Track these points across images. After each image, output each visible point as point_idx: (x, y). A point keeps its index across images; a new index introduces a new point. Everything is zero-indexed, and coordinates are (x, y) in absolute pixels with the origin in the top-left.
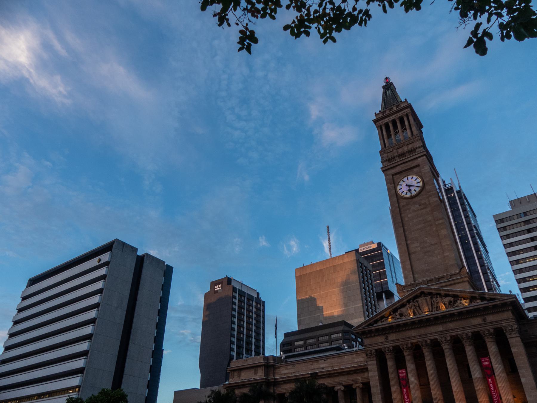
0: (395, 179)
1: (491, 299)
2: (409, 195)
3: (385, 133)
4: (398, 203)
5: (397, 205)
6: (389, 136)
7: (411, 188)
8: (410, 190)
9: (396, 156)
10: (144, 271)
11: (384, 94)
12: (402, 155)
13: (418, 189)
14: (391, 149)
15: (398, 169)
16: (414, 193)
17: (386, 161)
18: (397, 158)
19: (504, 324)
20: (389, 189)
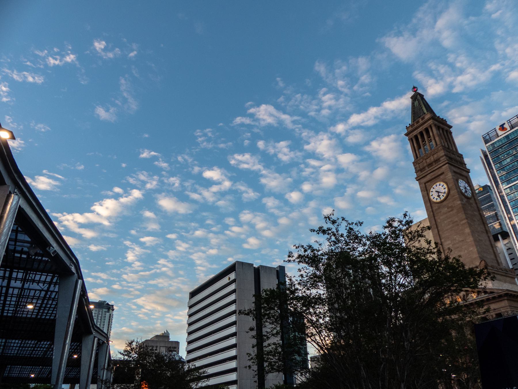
0: (427, 186)
1: (492, 293)
2: (439, 200)
3: (415, 145)
4: (432, 208)
5: (431, 210)
6: (419, 148)
7: (440, 194)
8: (439, 196)
9: (426, 166)
10: (262, 280)
11: (413, 104)
12: (430, 165)
13: (445, 195)
14: (421, 160)
15: (429, 177)
16: (442, 198)
17: (418, 171)
18: (427, 168)
19: (503, 310)
20: (423, 196)
